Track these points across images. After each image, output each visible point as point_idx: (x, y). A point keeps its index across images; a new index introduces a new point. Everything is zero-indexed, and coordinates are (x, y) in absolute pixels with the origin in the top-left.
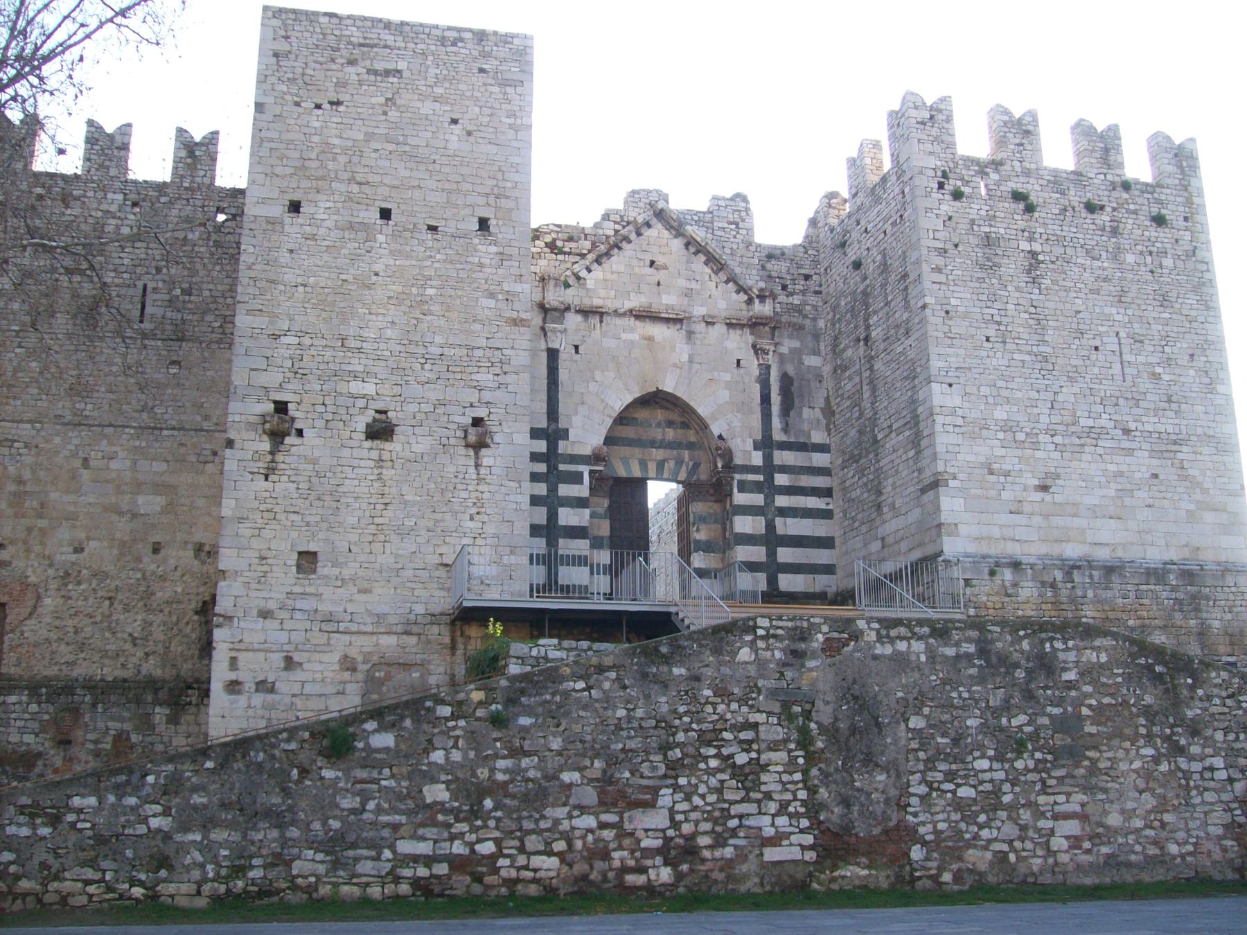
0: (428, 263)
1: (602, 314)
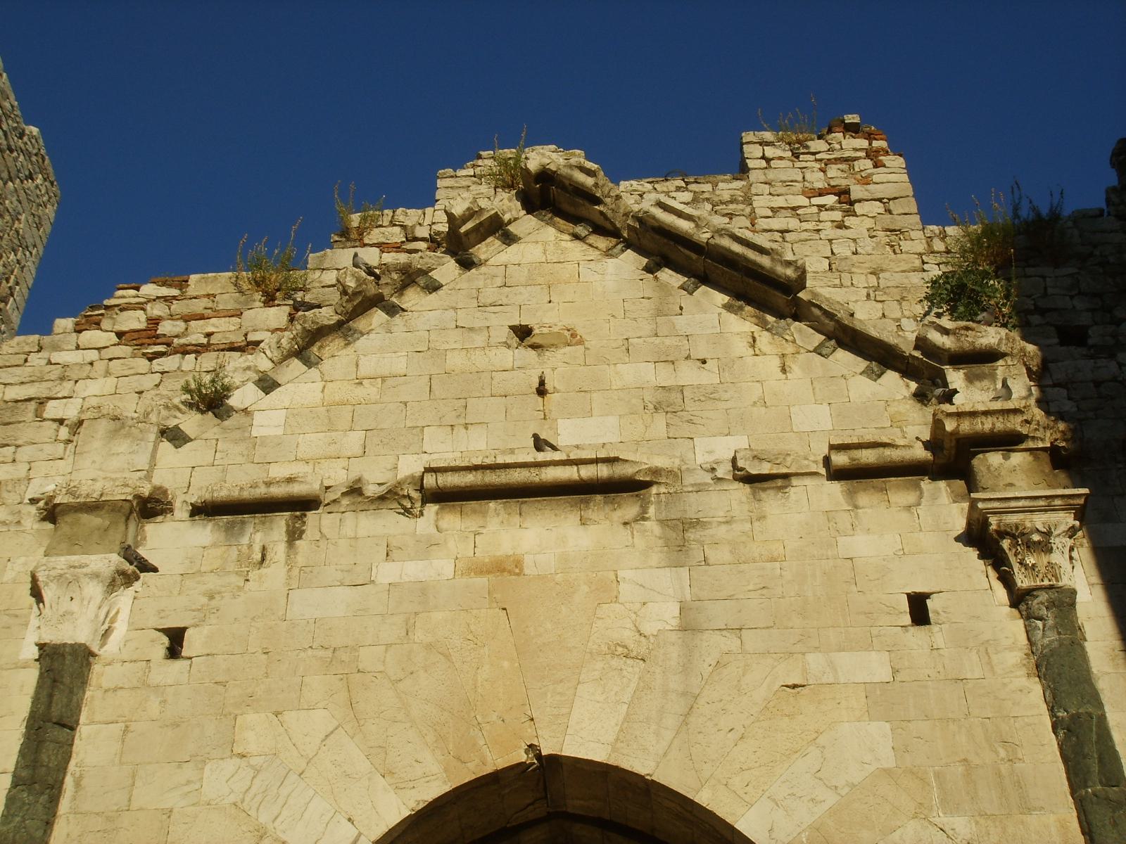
1: (304, 505)
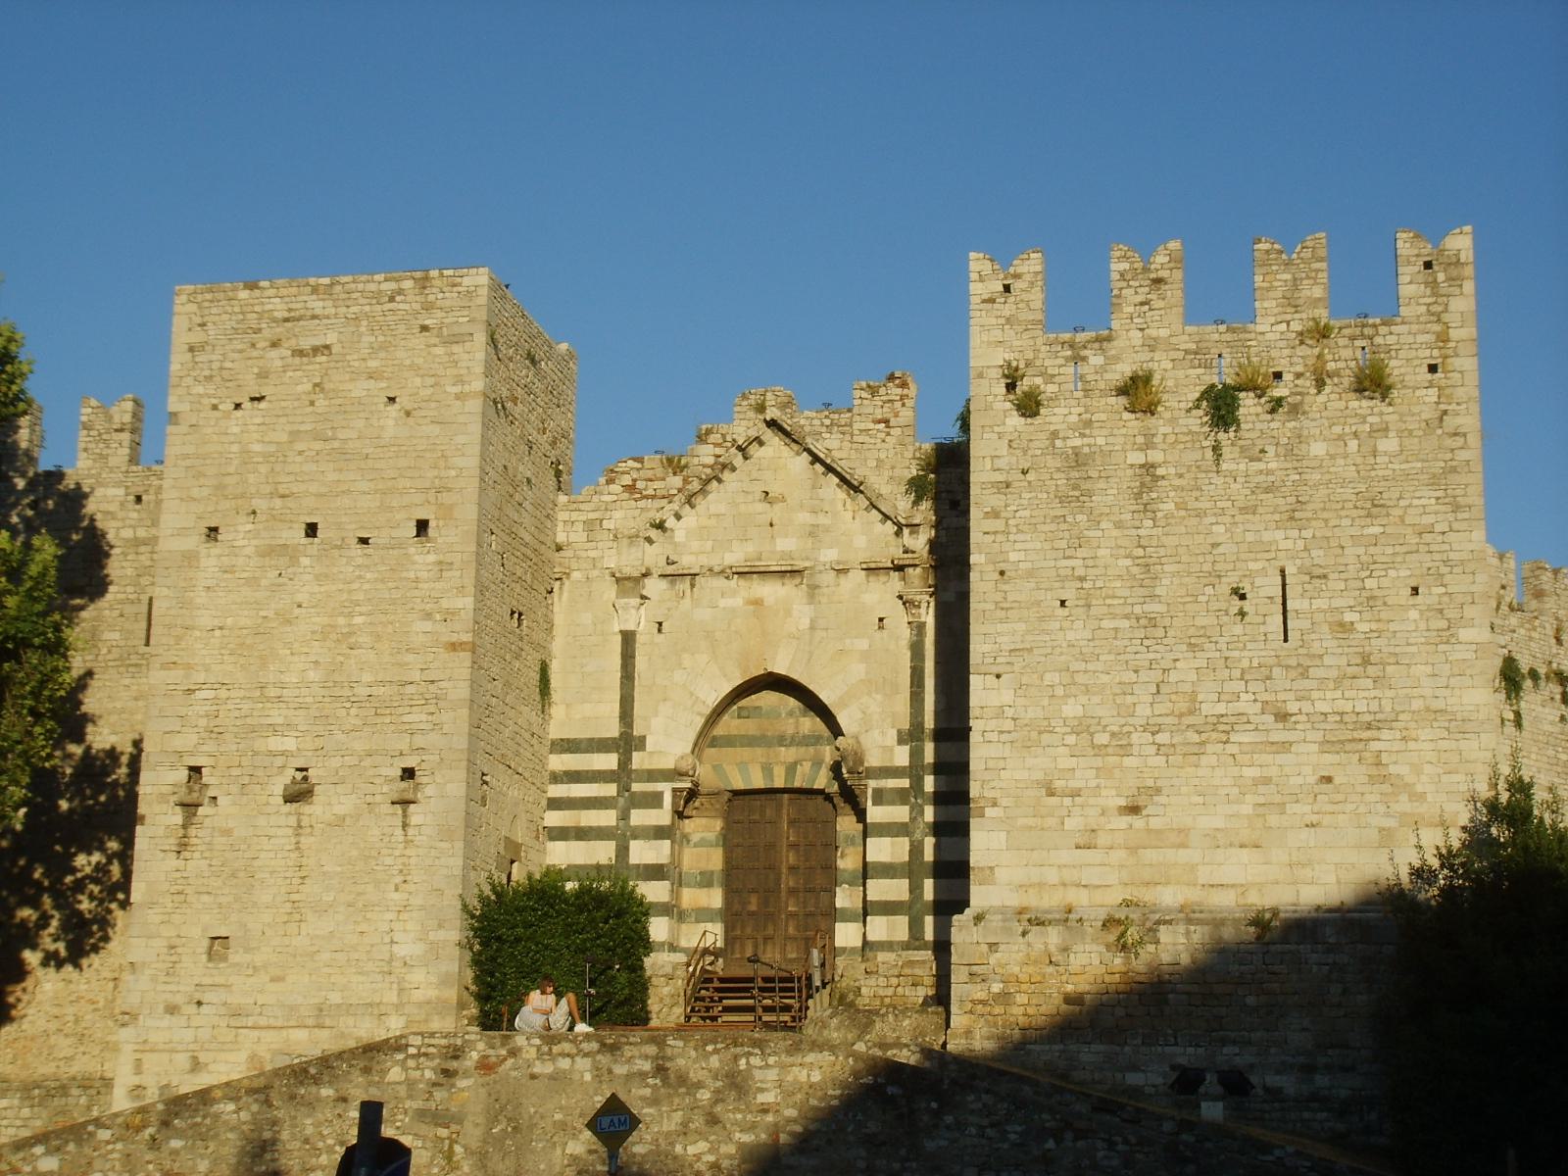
0: (355, 586)
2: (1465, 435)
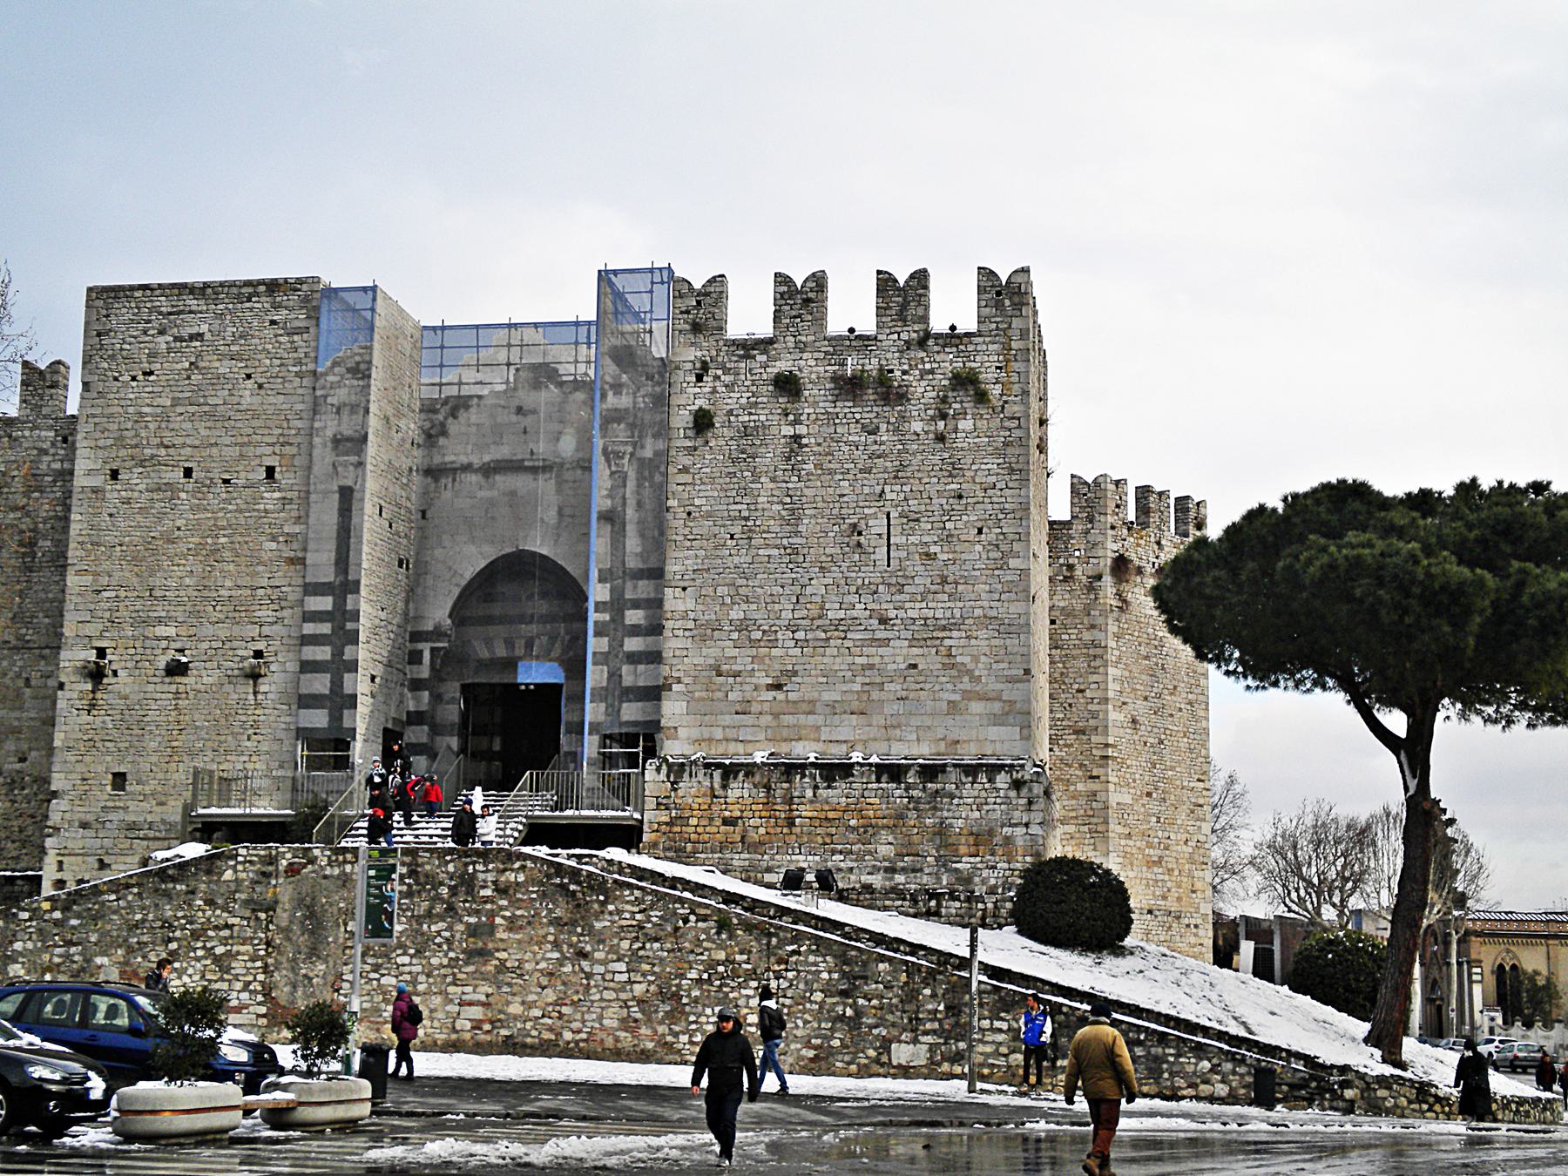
0: (221, 515)
2: (1019, 419)
